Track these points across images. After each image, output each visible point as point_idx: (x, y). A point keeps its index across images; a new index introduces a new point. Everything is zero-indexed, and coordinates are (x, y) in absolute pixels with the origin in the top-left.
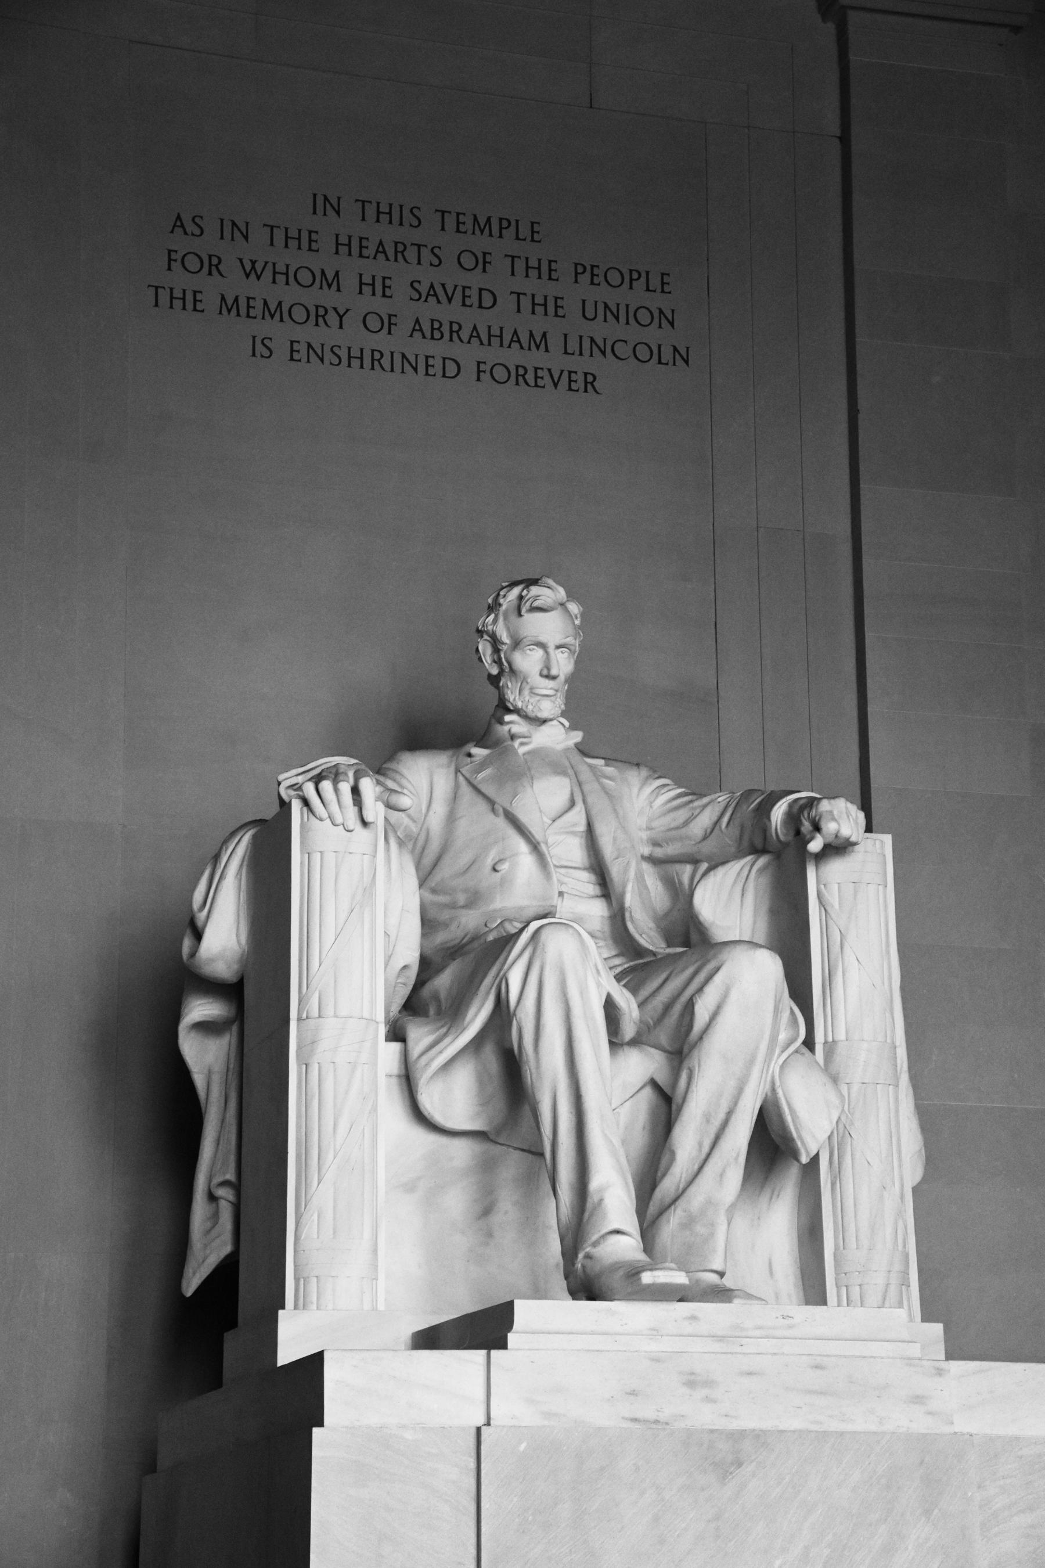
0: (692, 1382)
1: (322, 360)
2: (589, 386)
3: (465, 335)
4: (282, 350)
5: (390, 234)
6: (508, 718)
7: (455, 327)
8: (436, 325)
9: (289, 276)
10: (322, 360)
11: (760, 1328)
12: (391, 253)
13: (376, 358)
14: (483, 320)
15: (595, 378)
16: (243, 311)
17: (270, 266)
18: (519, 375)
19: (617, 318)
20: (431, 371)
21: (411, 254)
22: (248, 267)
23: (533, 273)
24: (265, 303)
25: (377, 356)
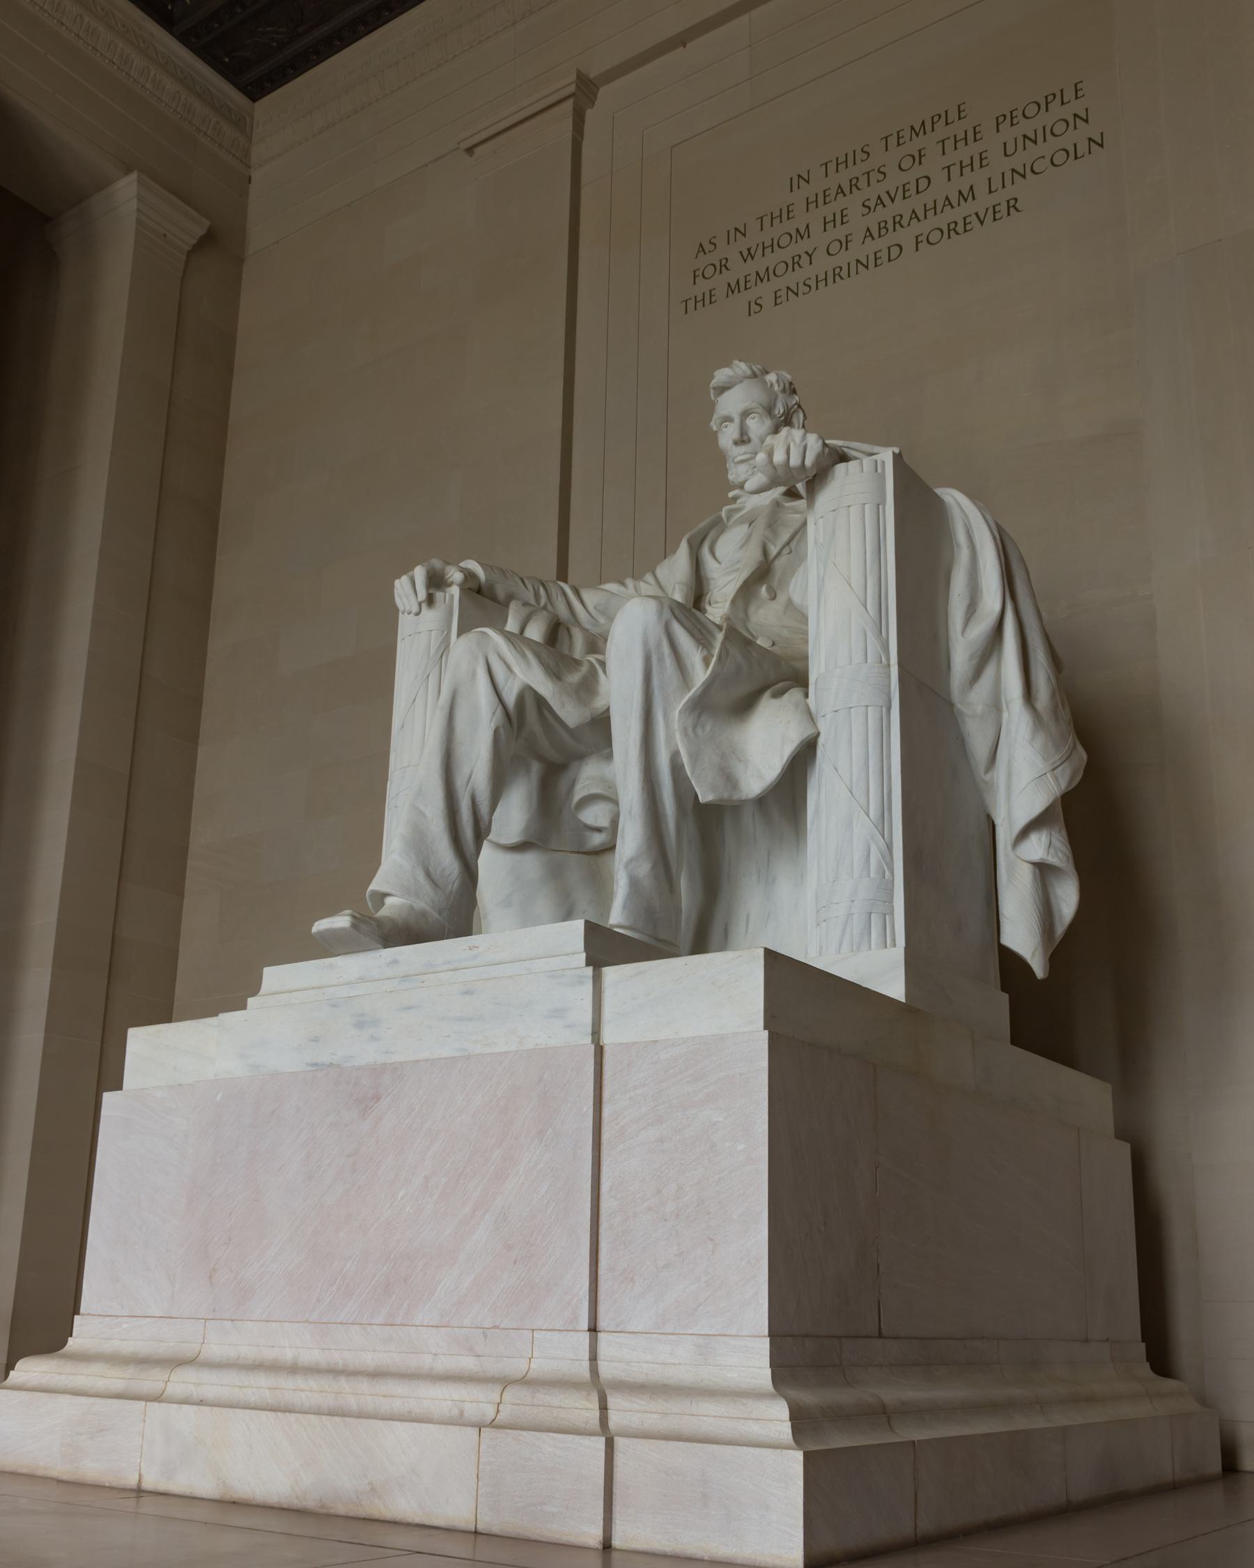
0: (360, 1025)
1: (797, 294)
2: (1012, 210)
3: (904, 222)
4: (768, 301)
5: (844, 177)
6: (731, 494)
7: (898, 219)
8: (883, 225)
9: (774, 245)
10: (797, 294)
11: (449, 962)
12: (847, 190)
13: (837, 274)
14: (917, 203)
15: (1016, 200)
16: (742, 288)
17: (760, 247)
18: (952, 229)
19: (1035, 142)
20: (879, 262)
21: (862, 183)
22: (745, 253)
23: (961, 144)
24: (757, 273)
25: (837, 271)
